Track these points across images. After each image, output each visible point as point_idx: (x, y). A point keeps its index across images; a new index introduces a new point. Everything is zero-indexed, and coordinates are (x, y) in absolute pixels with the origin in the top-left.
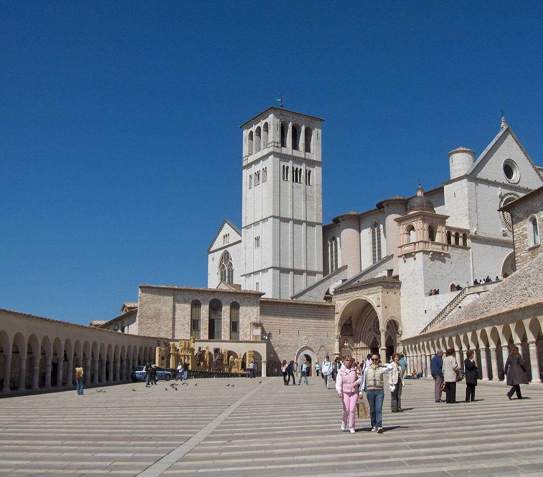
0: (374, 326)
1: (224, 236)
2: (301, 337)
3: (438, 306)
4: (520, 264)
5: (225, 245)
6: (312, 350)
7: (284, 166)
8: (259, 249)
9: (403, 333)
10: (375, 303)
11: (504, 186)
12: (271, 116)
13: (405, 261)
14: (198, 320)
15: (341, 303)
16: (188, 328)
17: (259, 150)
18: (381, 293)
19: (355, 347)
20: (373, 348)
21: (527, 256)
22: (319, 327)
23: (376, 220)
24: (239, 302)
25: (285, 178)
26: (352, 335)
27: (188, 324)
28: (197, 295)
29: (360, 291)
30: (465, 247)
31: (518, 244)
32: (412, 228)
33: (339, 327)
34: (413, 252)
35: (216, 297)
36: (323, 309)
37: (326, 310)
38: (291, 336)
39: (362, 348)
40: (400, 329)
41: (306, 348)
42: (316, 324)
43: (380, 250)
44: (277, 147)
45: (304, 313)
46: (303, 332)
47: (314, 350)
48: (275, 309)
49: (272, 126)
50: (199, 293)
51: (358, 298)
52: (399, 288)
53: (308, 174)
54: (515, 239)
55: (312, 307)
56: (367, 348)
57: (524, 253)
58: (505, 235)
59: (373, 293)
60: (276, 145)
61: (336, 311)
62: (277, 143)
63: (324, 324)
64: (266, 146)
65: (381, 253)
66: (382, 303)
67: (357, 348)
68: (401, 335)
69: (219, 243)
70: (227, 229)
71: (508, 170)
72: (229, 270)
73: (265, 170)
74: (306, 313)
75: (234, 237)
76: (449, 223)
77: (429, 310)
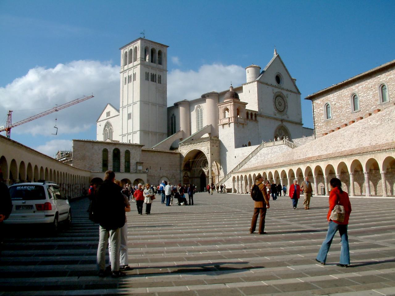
1: (107, 113)
2: (162, 171)
3: (243, 154)
4: (317, 130)
5: (108, 117)
7: (146, 73)
8: (130, 121)
11: (275, 87)
12: (139, 42)
13: (223, 128)
14: (106, 161)
15: (184, 150)
16: (101, 165)
17: (130, 62)
21: (323, 125)
24: (130, 150)
25: (147, 79)
27: (101, 163)
28: (106, 146)
30: (256, 120)
31: (316, 118)
32: (227, 110)
35: (117, 147)
37: (175, 155)
38: (156, 171)
41: (165, 177)
43: (202, 122)
44: (142, 61)
47: (169, 179)
49: (140, 49)
50: (107, 144)
53: (160, 77)
54: (315, 115)
55: (166, 153)
57: (321, 124)
58: (275, 115)
59: (204, 146)
60: (142, 59)
62: (143, 58)
64: (135, 60)
65: (202, 124)
66: (211, 152)
69: (104, 116)
70: (109, 108)
71: (278, 79)
72: (109, 132)
73: (134, 75)
75: (113, 112)
76: (248, 107)
77: (237, 156)
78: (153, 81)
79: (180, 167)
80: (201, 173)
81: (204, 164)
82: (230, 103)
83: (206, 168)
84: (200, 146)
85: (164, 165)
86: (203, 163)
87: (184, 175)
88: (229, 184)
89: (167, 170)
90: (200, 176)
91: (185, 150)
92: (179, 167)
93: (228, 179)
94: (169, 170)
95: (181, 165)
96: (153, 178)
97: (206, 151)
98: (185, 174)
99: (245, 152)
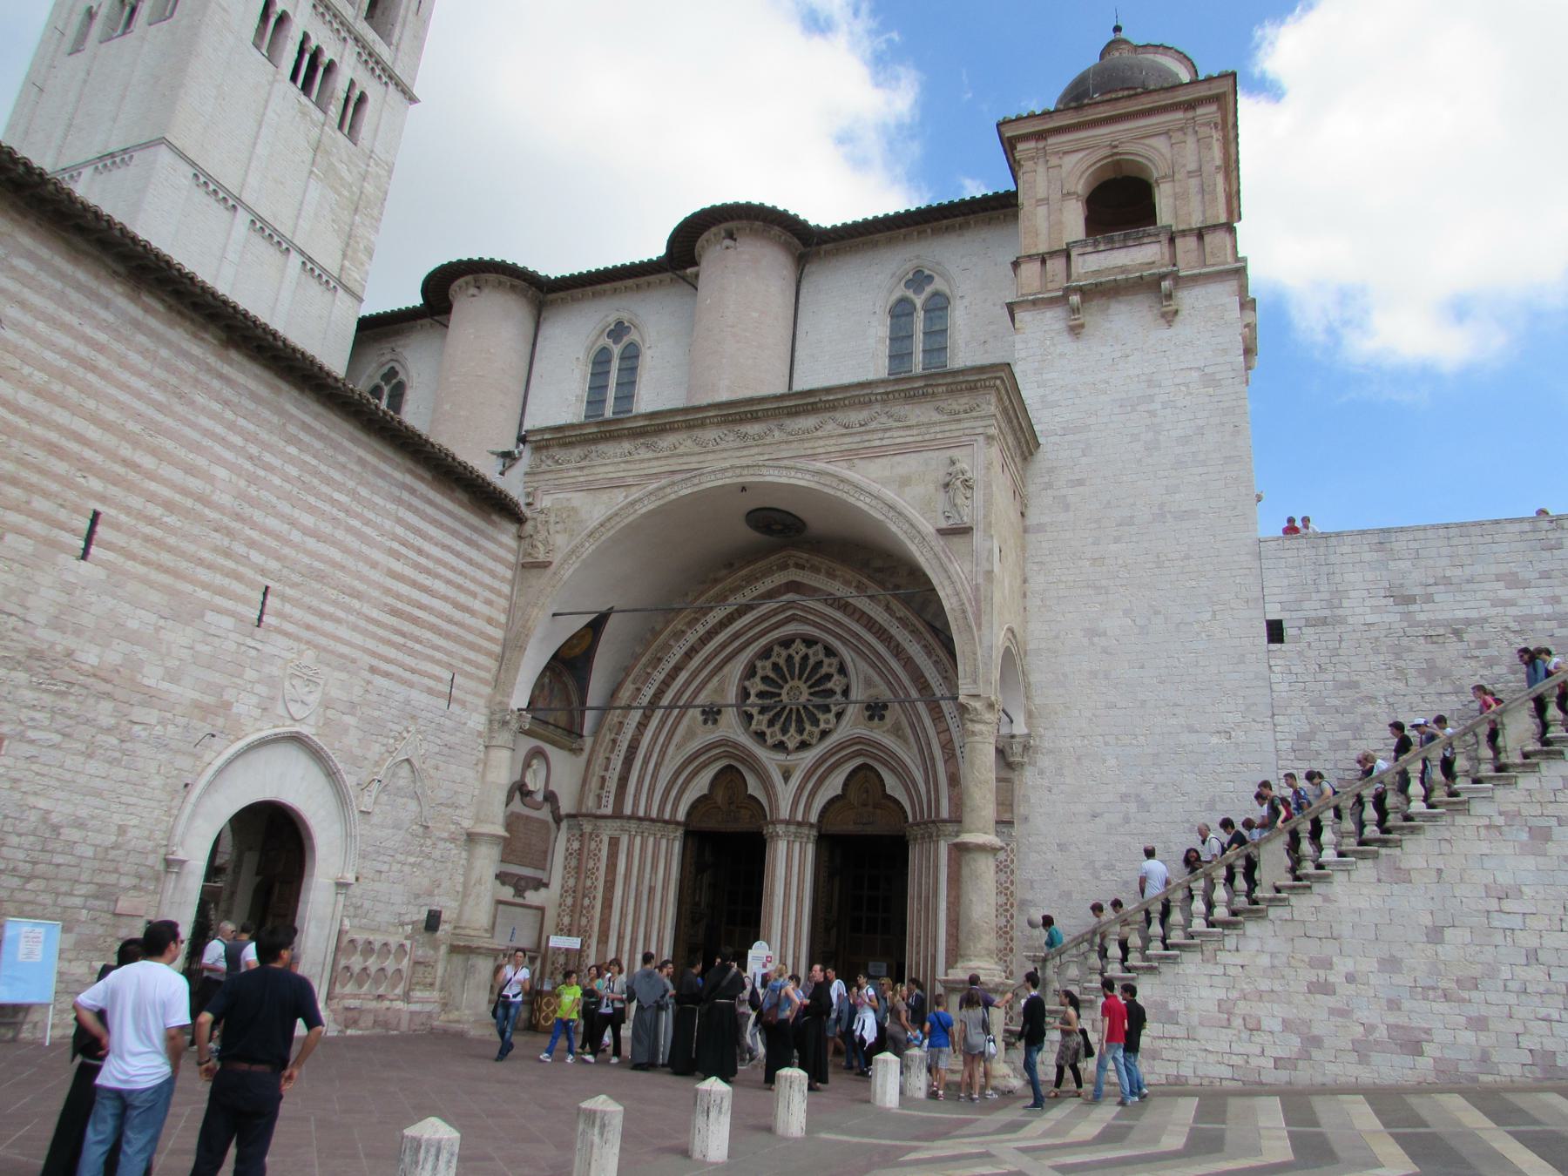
0: (745, 694)
2: (278, 646)
3: (1411, 600)
6: (331, 774)
9: (1044, 761)
13: (1075, 330)
22: (415, 621)
23: (625, 316)
26: (570, 734)
34: (1163, 277)
36: (461, 512)
42: (404, 589)
45: (337, 476)
46: (298, 613)
47: (350, 780)
48: (103, 314)
51: (748, 478)
59: (903, 450)
63: (447, 609)
74: (351, 484)
77: (1310, 623)
78: (306, 88)
79: (501, 683)
80: (701, 785)
81: (756, 686)
82: (1179, 115)
83: (792, 740)
84: (820, 446)
85: (321, 577)
86: (750, 672)
87: (517, 777)
88: (1328, 964)
89: (345, 665)
90: (681, 815)
91: (591, 488)
92: (492, 664)
93: (1302, 904)
94: (373, 670)
95: (512, 646)
96: (104, 712)
98: (527, 765)
99: (1447, 581)
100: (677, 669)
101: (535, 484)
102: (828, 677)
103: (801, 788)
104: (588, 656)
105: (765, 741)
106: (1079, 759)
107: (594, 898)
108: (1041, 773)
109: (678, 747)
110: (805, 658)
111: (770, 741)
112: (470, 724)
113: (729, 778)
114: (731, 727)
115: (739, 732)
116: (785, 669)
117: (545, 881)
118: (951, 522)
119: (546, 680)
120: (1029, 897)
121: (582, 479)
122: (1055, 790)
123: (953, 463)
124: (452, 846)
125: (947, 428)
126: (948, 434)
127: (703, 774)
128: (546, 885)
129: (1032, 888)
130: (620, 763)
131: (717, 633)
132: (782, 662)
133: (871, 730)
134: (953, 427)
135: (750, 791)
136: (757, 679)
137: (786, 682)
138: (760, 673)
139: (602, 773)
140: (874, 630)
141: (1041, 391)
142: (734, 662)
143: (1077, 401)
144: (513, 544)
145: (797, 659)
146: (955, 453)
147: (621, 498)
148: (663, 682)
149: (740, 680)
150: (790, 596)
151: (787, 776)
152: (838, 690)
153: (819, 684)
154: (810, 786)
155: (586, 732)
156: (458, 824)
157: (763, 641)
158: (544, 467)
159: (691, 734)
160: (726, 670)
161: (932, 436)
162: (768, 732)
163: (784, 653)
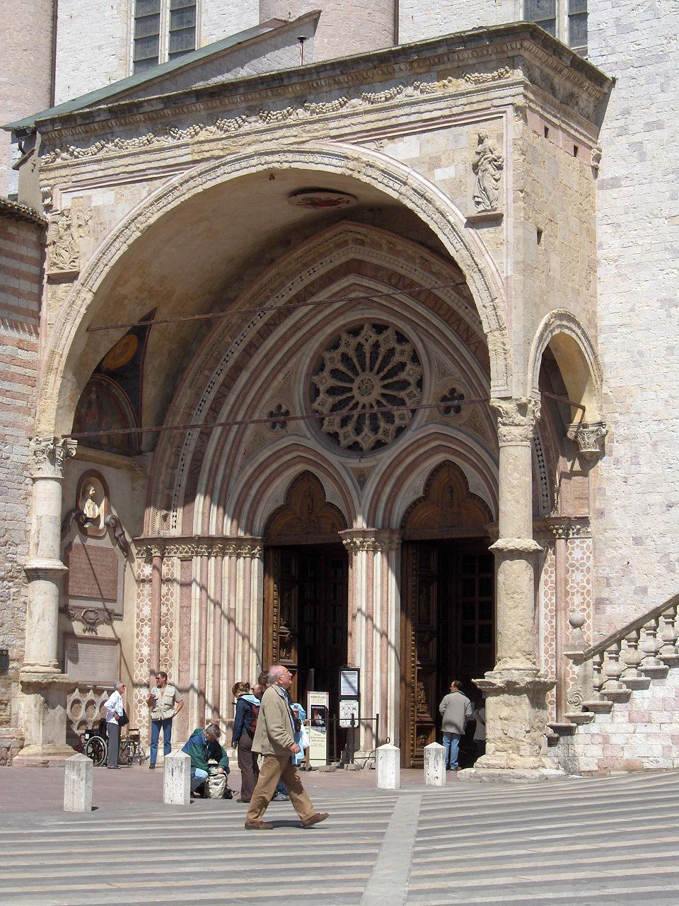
0: (314, 392)
9: (617, 449)
10: (442, 201)
18: (511, 126)
19: (148, 532)
20: (277, 548)
29: (302, 114)
33: (70, 376)
39: (225, 540)
40: (591, 411)
51: (275, 162)
52: (595, 119)
56: (239, 541)
59: (429, 125)
61: (55, 261)
67: (164, 543)
68: (589, 462)
81: (325, 382)
84: (348, 125)
86: (319, 367)
97: (454, 189)
100: (237, 369)
101: (52, 182)
102: (402, 366)
103: (377, 494)
104: (135, 366)
105: (339, 442)
106: (655, 445)
107: (172, 625)
108: (617, 462)
109: (249, 456)
110: (376, 345)
111: (344, 443)
112: (14, 458)
113: (306, 486)
114: (301, 434)
115: (309, 435)
116: (355, 360)
117: (117, 611)
118: (481, 207)
119: (94, 396)
120: (605, 595)
121: (100, 174)
122: (630, 481)
123: (481, 141)
124: (11, 584)
125: (475, 99)
126: (475, 107)
127: (278, 482)
128: (120, 616)
129: (608, 585)
130: (185, 478)
131: (276, 325)
132: (352, 353)
133: (447, 424)
134: (481, 97)
135: (328, 499)
136: (326, 373)
137: (357, 374)
138: (329, 367)
139: (166, 492)
140: (442, 312)
141: (617, 13)
142: (299, 354)
143: (655, 23)
144: (34, 253)
145: (367, 348)
146: (483, 128)
147: (144, 194)
148: (223, 384)
149: (307, 375)
150: (351, 279)
151: (362, 479)
152: (412, 380)
153: (392, 375)
154: (388, 489)
155: (143, 447)
156: (13, 561)
157: (329, 330)
158: (59, 161)
159: (260, 443)
160: (290, 365)
161: (459, 110)
162: (341, 432)
163: (353, 342)
